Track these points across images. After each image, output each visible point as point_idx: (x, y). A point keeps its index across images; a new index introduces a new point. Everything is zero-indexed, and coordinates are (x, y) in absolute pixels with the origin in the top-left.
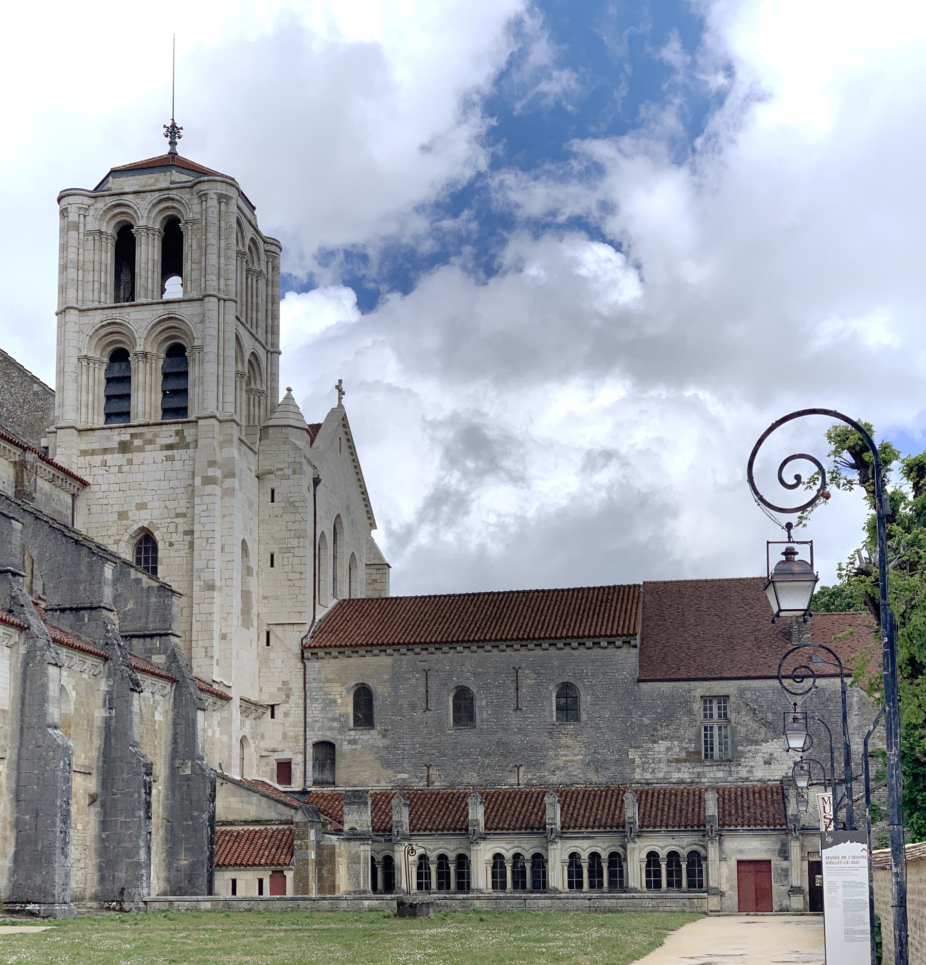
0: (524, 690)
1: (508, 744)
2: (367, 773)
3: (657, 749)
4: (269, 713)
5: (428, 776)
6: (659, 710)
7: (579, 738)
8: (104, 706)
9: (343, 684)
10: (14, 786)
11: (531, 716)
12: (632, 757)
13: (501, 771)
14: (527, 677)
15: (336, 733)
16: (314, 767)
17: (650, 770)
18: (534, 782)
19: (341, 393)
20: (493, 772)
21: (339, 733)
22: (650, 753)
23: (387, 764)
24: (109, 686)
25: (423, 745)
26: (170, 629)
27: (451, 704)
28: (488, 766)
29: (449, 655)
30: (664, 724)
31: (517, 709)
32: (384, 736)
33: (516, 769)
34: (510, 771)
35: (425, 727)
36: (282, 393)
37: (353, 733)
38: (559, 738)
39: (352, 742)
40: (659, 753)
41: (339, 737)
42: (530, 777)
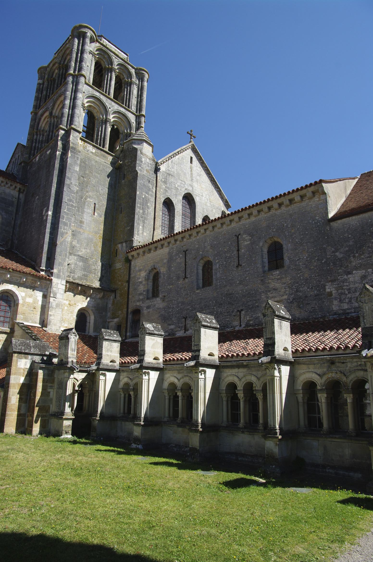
0: (243, 251)
1: (233, 294)
3: (351, 279)
5: (185, 325)
6: (351, 243)
7: (284, 281)
11: (248, 269)
12: (328, 290)
13: (229, 316)
14: (244, 240)
15: (141, 303)
17: (347, 300)
18: (251, 322)
20: (223, 317)
21: (142, 302)
22: (345, 284)
25: (183, 303)
27: (200, 272)
28: (221, 313)
29: (198, 237)
30: (357, 255)
31: (239, 265)
32: (164, 301)
33: (238, 313)
34: (234, 316)
35: (184, 290)
38: (269, 283)
39: (148, 307)
40: (355, 282)
41: (142, 305)
42: (248, 319)
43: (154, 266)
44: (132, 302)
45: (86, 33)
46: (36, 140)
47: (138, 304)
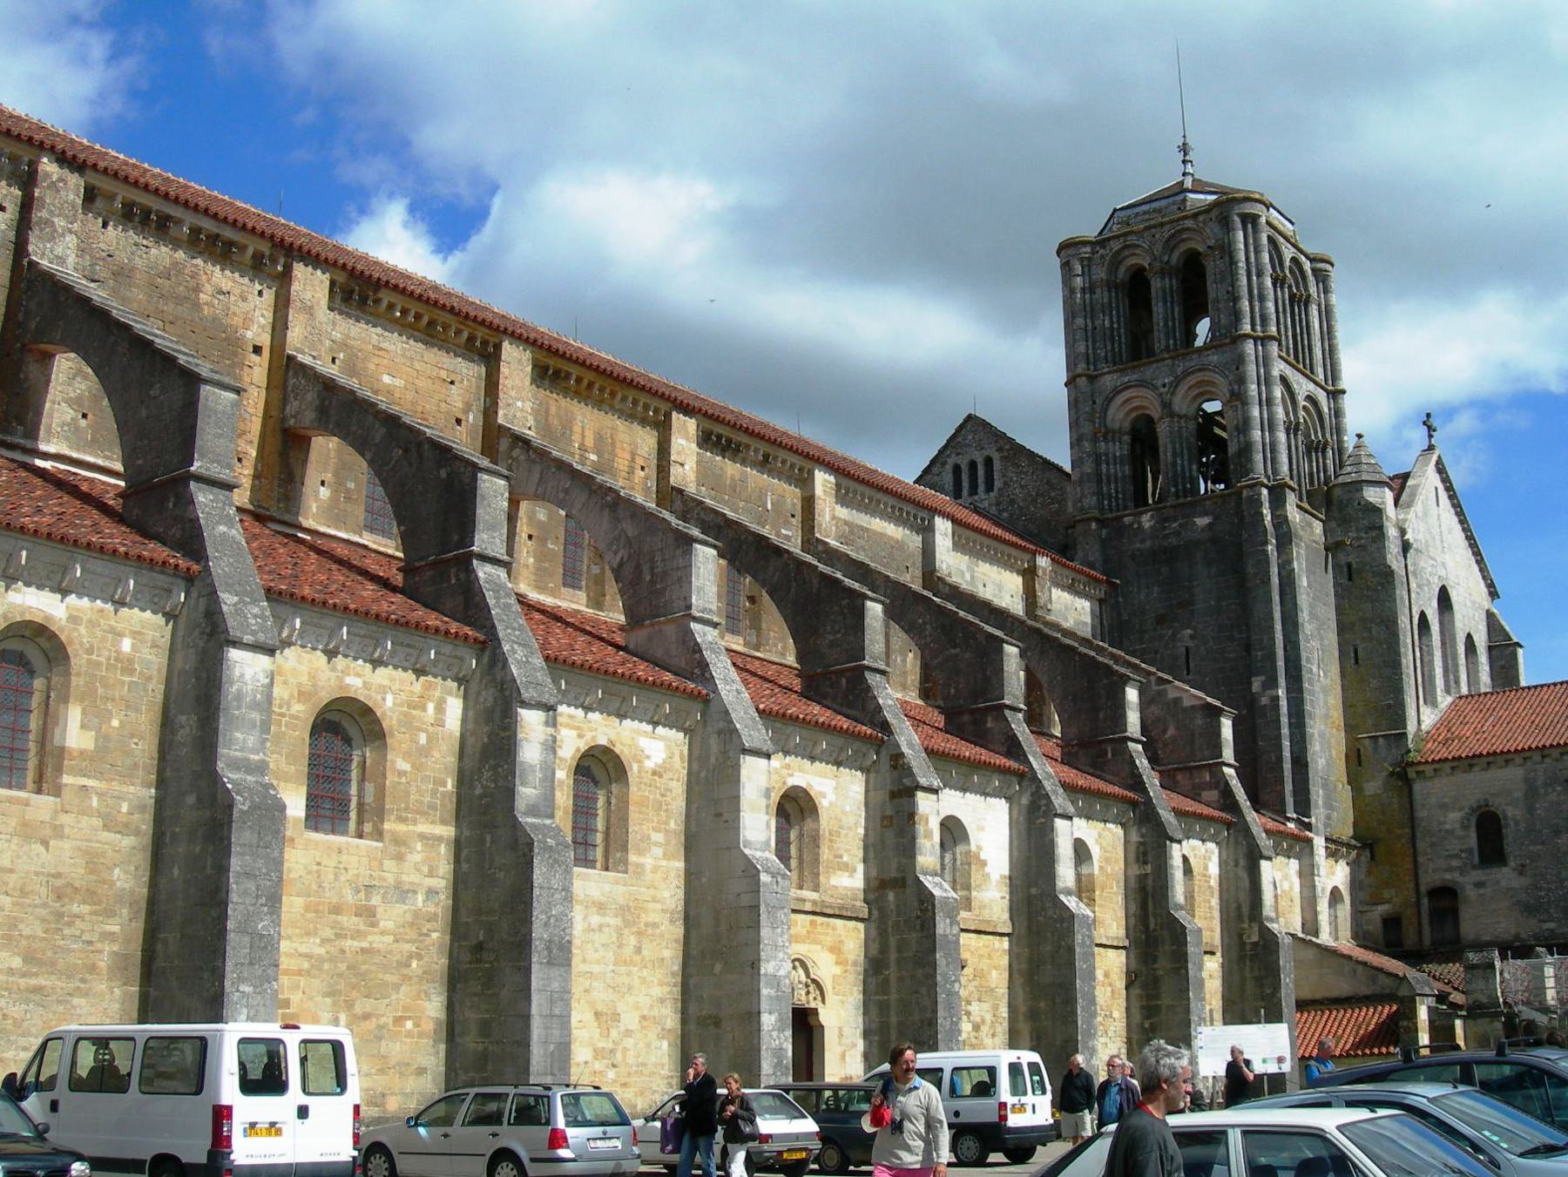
2: (1502, 925)
4: (1367, 853)
8: (1138, 860)
9: (1460, 810)
10: (1024, 966)
16: (1431, 923)
19: (1431, 429)
23: (1529, 909)
24: (1142, 836)
26: (1221, 757)
32: (1521, 873)
36: (1349, 441)
37: (1479, 872)
39: (1480, 885)
41: (1460, 880)
43: (1486, 800)
44: (1426, 872)
45: (1259, 216)
46: (1107, 455)
47: (1448, 876)
